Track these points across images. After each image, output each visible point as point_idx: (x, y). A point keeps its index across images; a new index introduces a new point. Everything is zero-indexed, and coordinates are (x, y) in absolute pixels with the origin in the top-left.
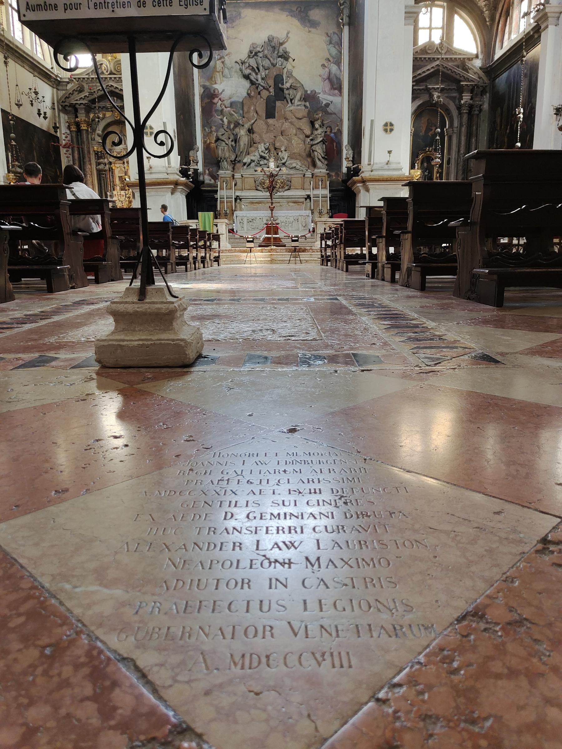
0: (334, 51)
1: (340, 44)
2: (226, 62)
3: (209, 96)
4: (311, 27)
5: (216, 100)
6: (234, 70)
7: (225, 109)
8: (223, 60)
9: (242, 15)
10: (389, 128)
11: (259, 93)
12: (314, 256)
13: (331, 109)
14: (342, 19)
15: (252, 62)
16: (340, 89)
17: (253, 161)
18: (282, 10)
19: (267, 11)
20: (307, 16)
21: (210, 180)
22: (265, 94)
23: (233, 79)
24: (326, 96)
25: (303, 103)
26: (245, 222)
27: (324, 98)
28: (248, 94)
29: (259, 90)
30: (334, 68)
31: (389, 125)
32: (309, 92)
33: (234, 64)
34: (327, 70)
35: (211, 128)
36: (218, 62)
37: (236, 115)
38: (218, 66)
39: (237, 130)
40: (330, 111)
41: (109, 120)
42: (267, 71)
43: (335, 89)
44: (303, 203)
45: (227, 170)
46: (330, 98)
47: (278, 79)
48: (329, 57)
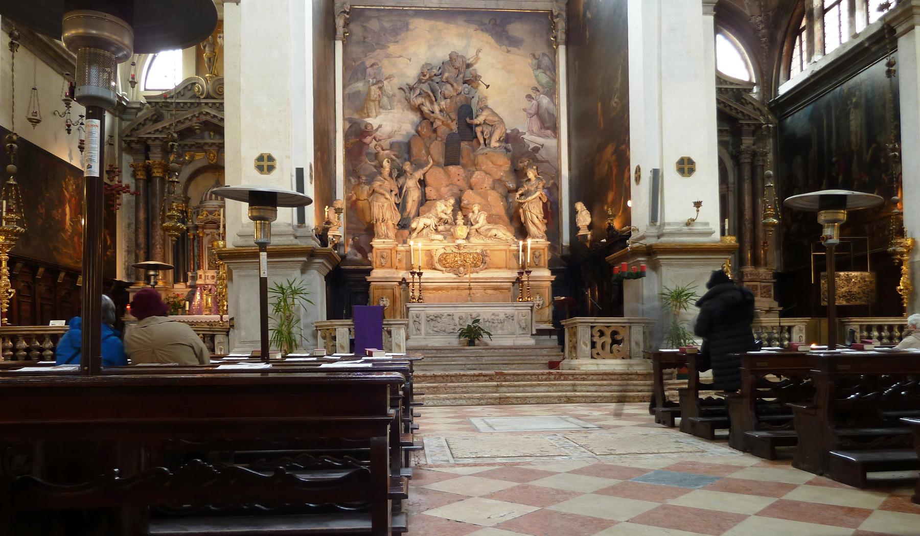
0: (544, 79)
1: (553, 68)
2: (385, 87)
3: (358, 136)
4: (510, 45)
5: (368, 139)
6: (396, 98)
7: (382, 152)
8: (380, 85)
9: (411, 27)
10: (686, 167)
11: (435, 131)
12: (579, 388)
13: (542, 154)
14: (555, 37)
15: (425, 87)
16: (555, 128)
17: (426, 226)
18: (468, 21)
19: (447, 22)
20: (504, 31)
21: (356, 255)
22: (443, 131)
23: (395, 111)
24: (533, 138)
25: (503, 144)
26: (423, 322)
27: (532, 139)
28: (417, 132)
29: (435, 126)
30: (545, 101)
31: (686, 161)
32: (509, 131)
33: (397, 92)
34: (534, 102)
35: (359, 177)
36: (373, 88)
37: (398, 161)
38: (372, 93)
39: (401, 181)
40: (540, 158)
41: (197, 165)
42: (448, 100)
43: (548, 128)
44: (509, 289)
45: (387, 237)
46: (540, 140)
47: (465, 113)
48: (536, 85)
